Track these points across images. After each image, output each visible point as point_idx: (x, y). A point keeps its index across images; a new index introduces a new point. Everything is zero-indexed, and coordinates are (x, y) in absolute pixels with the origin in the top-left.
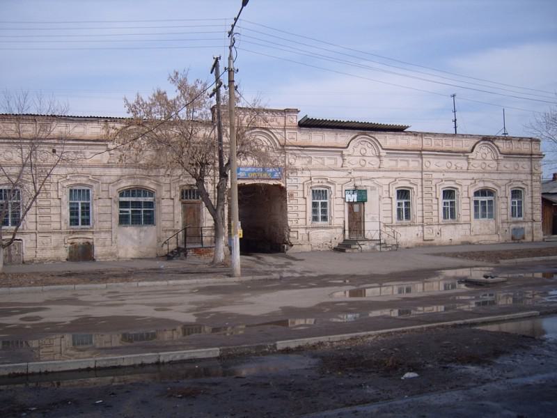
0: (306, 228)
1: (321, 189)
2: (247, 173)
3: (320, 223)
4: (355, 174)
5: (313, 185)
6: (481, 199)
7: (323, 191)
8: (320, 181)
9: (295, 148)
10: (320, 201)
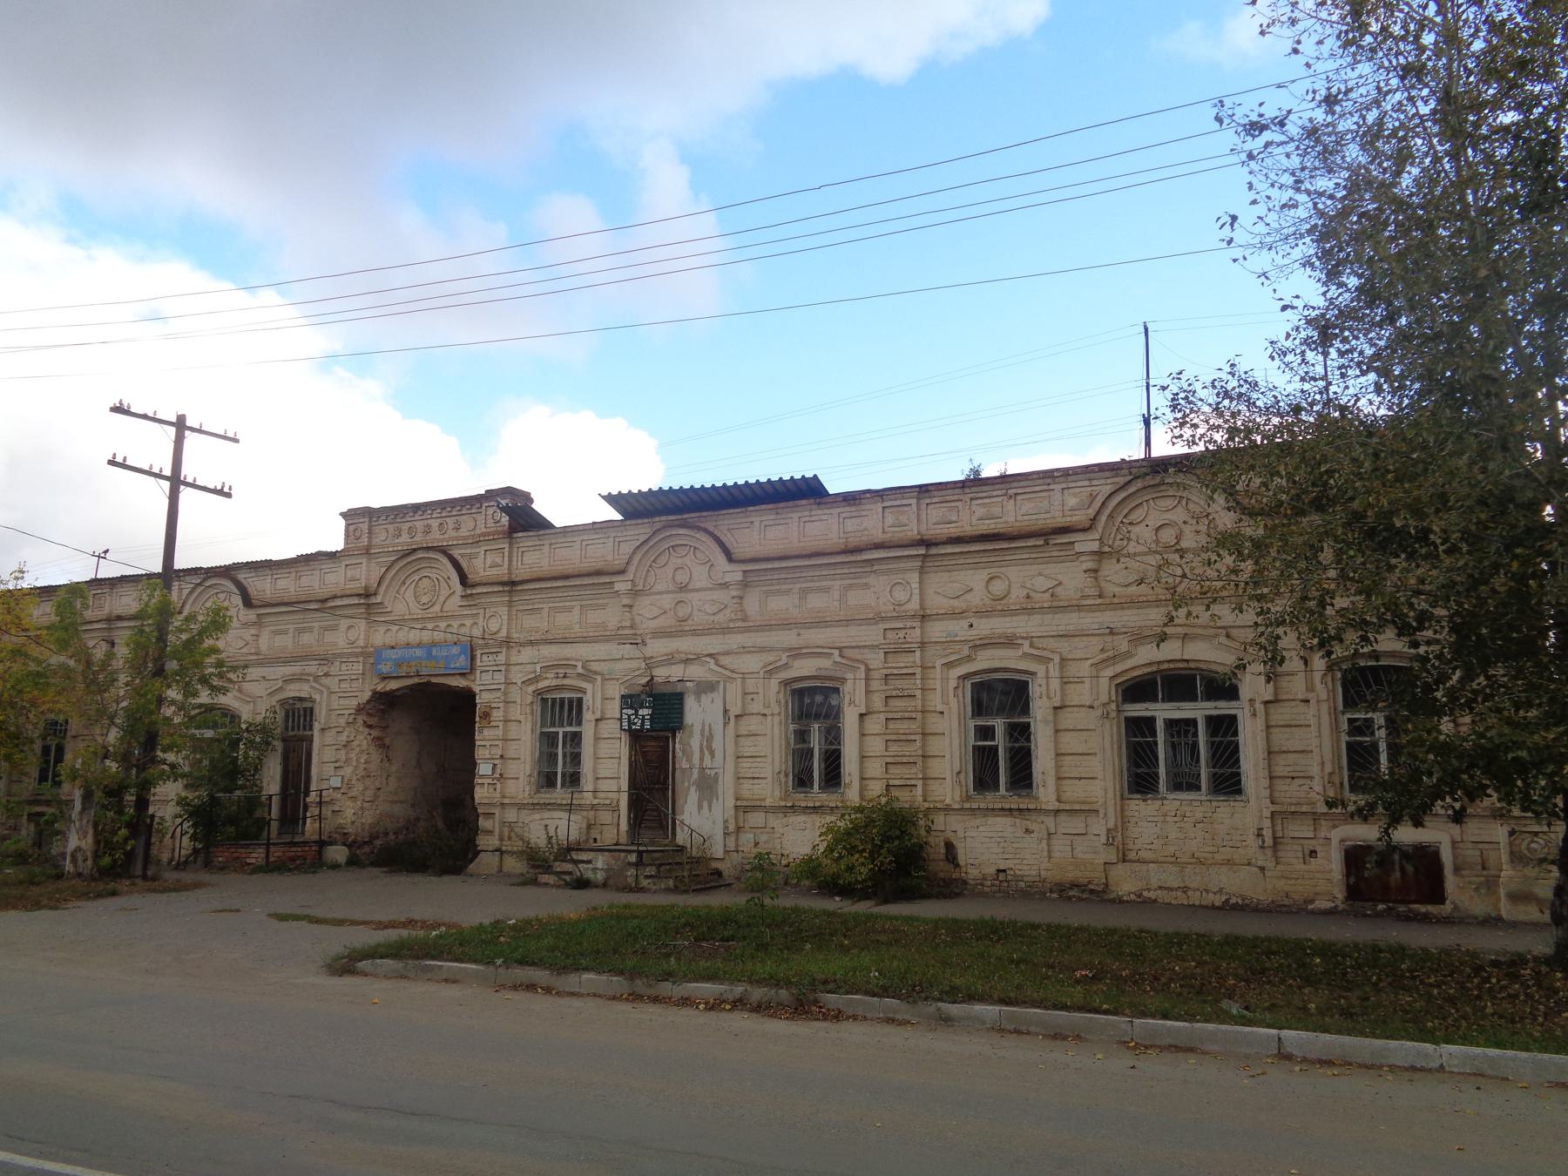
0: (521, 806)
1: (567, 695)
2: (399, 664)
3: (560, 794)
4: (657, 648)
5: (541, 685)
6: (1162, 712)
7: (571, 701)
9: (490, 589)
10: (561, 731)
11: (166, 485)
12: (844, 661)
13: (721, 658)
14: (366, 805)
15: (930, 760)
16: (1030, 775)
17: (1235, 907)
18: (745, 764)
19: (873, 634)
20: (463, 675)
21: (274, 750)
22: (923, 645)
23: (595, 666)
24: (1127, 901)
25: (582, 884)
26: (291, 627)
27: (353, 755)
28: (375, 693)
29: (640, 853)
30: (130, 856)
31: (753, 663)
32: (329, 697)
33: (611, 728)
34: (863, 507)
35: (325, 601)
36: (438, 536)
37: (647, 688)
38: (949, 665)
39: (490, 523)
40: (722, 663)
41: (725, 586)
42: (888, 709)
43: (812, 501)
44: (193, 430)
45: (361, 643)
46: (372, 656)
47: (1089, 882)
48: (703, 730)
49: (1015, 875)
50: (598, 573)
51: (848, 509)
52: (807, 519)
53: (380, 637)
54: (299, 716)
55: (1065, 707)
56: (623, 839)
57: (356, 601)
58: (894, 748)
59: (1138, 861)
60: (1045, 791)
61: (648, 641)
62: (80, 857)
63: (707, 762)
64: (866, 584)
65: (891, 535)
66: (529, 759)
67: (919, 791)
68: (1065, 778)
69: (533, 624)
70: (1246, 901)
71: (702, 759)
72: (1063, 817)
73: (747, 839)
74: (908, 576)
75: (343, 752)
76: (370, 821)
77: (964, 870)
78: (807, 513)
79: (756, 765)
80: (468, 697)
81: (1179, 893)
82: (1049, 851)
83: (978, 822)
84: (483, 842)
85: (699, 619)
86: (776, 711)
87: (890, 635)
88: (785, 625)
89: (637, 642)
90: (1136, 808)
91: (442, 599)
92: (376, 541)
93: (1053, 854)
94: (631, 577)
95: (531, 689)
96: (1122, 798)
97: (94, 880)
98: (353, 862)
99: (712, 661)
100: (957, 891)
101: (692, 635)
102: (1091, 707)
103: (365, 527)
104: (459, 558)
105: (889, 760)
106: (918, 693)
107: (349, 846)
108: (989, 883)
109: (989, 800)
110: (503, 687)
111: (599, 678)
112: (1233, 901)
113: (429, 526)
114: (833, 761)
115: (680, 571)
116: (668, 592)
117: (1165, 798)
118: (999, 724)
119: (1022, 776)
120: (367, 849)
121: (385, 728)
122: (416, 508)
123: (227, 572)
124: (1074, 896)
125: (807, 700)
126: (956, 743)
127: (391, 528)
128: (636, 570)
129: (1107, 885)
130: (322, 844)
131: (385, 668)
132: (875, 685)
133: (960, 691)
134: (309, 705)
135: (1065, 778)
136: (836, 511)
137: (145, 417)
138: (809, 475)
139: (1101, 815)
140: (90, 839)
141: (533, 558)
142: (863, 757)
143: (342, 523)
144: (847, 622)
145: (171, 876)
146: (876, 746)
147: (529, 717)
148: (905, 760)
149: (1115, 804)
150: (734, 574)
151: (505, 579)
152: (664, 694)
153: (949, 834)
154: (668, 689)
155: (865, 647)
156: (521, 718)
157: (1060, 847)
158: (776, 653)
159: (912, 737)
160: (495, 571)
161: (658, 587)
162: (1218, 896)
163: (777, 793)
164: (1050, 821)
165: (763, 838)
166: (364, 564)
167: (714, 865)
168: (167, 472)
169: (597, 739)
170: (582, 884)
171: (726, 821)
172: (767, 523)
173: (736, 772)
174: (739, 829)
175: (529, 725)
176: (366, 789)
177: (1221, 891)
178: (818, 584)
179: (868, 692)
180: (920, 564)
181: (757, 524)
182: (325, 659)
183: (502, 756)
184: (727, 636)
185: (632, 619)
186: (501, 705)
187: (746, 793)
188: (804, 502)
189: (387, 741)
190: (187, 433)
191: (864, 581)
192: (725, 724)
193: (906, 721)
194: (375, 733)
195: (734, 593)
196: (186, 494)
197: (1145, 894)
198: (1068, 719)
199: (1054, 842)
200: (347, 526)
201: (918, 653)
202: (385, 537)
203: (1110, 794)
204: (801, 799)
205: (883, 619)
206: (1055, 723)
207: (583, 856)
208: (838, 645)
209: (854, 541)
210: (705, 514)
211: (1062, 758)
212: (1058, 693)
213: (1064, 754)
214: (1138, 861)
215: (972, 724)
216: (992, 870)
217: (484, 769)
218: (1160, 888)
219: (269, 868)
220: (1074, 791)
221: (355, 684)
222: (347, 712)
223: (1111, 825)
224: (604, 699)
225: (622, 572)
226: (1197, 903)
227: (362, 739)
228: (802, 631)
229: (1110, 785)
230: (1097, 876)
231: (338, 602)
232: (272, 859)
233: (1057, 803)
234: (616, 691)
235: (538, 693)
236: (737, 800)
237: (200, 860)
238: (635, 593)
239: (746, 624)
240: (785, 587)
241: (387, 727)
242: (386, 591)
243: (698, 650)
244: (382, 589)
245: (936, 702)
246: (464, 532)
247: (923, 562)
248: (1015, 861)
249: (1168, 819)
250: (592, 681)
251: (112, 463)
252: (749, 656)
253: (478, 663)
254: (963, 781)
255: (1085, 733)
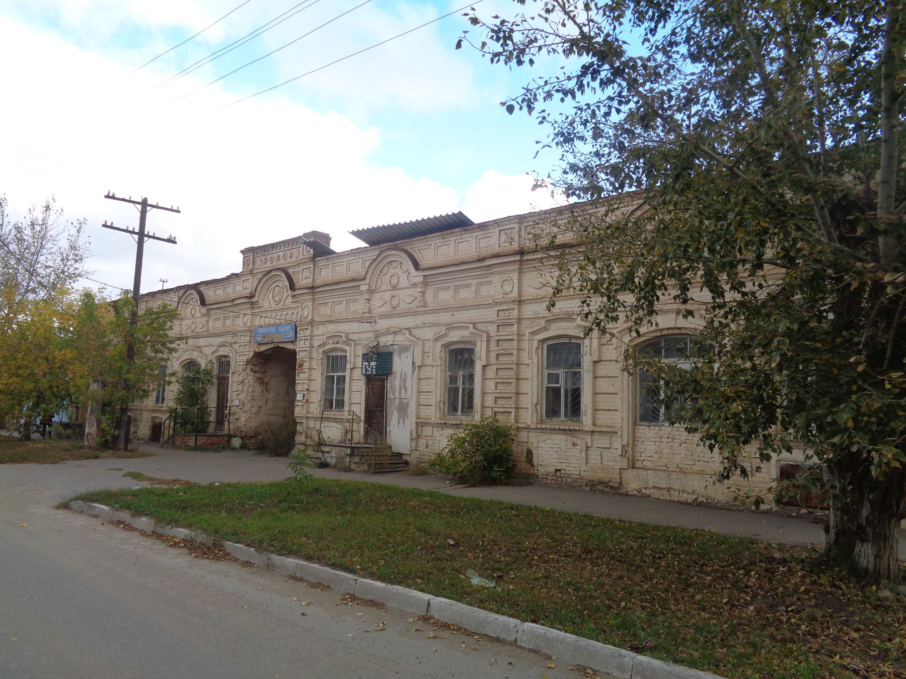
0: (316, 419)
1: (339, 354)
4: (382, 324)
8: (336, 339)
10: (336, 375)
11: (136, 237)
12: (475, 331)
13: (412, 330)
14: (252, 415)
15: (521, 396)
16: (579, 408)
17: (701, 505)
18: (423, 396)
19: (491, 314)
20: (292, 342)
21: (212, 384)
22: (519, 320)
23: (352, 337)
24: (631, 495)
25: (324, 465)
26: (222, 316)
27: (245, 388)
28: (255, 353)
29: (352, 448)
30: (115, 438)
31: (429, 333)
32: (236, 355)
33: (358, 374)
34: (490, 231)
35: (232, 301)
36: (283, 262)
37: (374, 349)
38: (534, 333)
39: (305, 252)
40: (413, 333)
41: (415, 285)
42: (498, 362)
43: (461, 229)
44: (153, 206)
45: (249, 324)
46: (251, 331)
47: (610, 481)
48: (401, 375)
49: (566, 474)
50: (353, 280)
51: (481, 233)
52: (459, 241)
53: (258, 321)
54: (224, 363)
55: (602, 361)
56: (362, 441)
57: (245, 300)
58: (500, 387)
59: (642, 468)
60: (586, 419)
61: (378, 321)
62: (90, 438)
63: (403, 395)
64: (490, 281)
65: (502, 248)
66: (320, 391)
67: (512, 416)
68: (599, 410)
69: (325, 311)
70: (709, 501)
71: (400, 393)
72: (596, 436)
73: (422, 442)
74: (511, 275)
75: (241, 386)
76: (254, 425)
77: (536, 468)
78: (459, 237)
79: (428, 397)
80: (293, 353)
81: (665, 492)
82: (587, 459)
83: (546, 437)
84: (300, 438)
85: (403, 307)
86: (439, 363)
87: (501, 313)
88: (446, 309)
89: (371, 320)
90: (643, 431)
91: (284, 298)
92: (256, 266)
93: (590, 461)
94: (368, 282)
95: (322, 350)
96: (635, 424)
97: (97, 449)
98: (243, 447)
99: (407, 332)
100: (532, 482)
101: (399, 317)
102: (617, 361)
103: (251, 258)
104: (291, 274)
105: (497, 395)
106: (515, 352)
107: (242, 439)
108: (550, 478)
109: (555, 423)
110: (308, 349)
111: (352, 343)
112: (700, 500)
113: (279, 256)
114: (470, 395)
115: (393, 278)
116: (388, 291)
117: (663, 426)
118: (561, 372)
119: (575, 409)
120: (253, 440)
121: (264, 373)
122: (273, 246)
123: (195, 287)
124: (598, 490)
125: (460, 357)
126: (535, 384)
127: (263, 258)
128: (371, 277)
129: (621, 483)
130: (230, 436)
131: (259, 339)
132: (493, 346)
133: (540, 351)
134: (228, 359)
135: (599, 410)
136: (474, 235)
137: (124, 200)
138: (457, 212)
139: (619, 436)
140: (94, 429)
141: (327, 273)
142: (484, 393)
143: (241, 256)
144: (478, 306)
145: (143, 448)
146: (490, 386)
147: (320, 367)
148: (506, 395)
149: (628, 428)
150: (417, 277)
151: (310, 285)
152: (383, 353)
153: (530, 445)
154: (385, 350)
155: (488, 322)
156: (316, 367)
157: (594, 455)
158: (439, 327)
159: (510, 381)
160: (306, 281)
161: (383, 288)
162: (690, 496)
163: (438, 415)
164: (588, 438)
165: (431, 443)
166: (250, 281)
167: (405, 458)
168: (137, 230)
169: (351, 380)
170: (324, 465)
171: (411, 431)
172: (439, 245)
173: (418, 401)
174: (418, 436)
175: (320, 371)
176: (252, 407)
177: (693, 492)
178: (464, 283)
179: (488, 351)
180: (518, 266)
181: (433, 245)
182: (235, 334)
183: (307, 390)
184: (416, 317)
185: (370, 308)
186: (307, 360)
187: (423, 415)
188: (457, 230)
189: (266, 380)
190: (149, 208)
191: (489, 279)
192: (413, 371)
193: (508, 370)
194: (258, 375)
195: (420, 290)
196: (148, 243)
197: (643, 491)
198: (602, 369)
199: (590, 453)
200: (244, 258)
201: (516, 326)
202: (263, 265)
203: (625, 421)
204: (451, 420)
205: (497, 304)
206: (594, 372)
207: (326, 449)
208: (473, 321)
209: (484, 254)
210: (406, 241)
211: (598, 396)
212: (596, 351)
213: (599, 394)
214: (642, 468)
215: (546, 372)
216: (552, 470)
217: (299, 397)
218: (654, 487)
219: (197, 448)
220: (604, 419)
221: (247, 348)
222: (242, 363)
223: (625, 443)
224: (356, 356)
225: (364, 279)
226: (676, 499)
227: (250, 379)
228: (454, 313)
229: (625, 414)
230: (615, 477)
231: (238, 302)
232: (198, 444)
233: (592, 426)
234: (360, 351)
235: (325, 352)
236: (418, 418)
237: (171, 442)
238: (371, 292)
239: (425, 309)
240: (446, 285)
241: (266, 372)
242: (259, 295)
243: (402, 326)
244: (257, 294)
245: (525, 358)
246: (294, 259)
247: (521, 265)
248: (565, 464)
249: (663, 440)
250: (350, 345)
251: (105, 226)
252: (427, 329)
253: (298, 335)
254: (539, 409)
255: (613, 379)
